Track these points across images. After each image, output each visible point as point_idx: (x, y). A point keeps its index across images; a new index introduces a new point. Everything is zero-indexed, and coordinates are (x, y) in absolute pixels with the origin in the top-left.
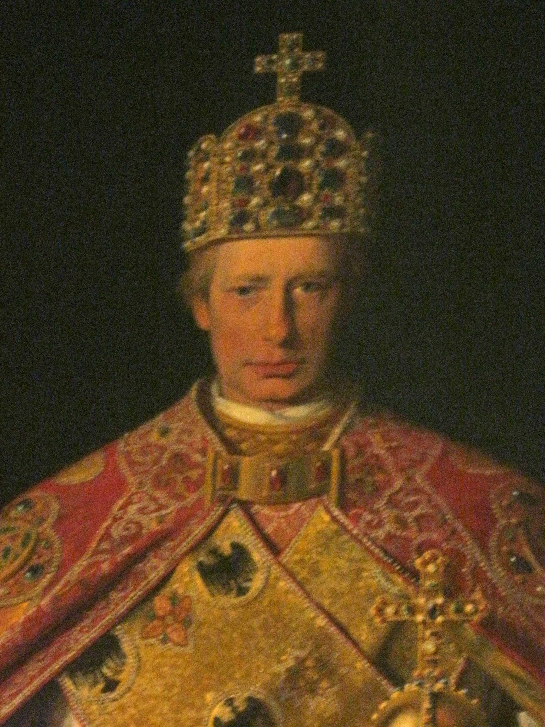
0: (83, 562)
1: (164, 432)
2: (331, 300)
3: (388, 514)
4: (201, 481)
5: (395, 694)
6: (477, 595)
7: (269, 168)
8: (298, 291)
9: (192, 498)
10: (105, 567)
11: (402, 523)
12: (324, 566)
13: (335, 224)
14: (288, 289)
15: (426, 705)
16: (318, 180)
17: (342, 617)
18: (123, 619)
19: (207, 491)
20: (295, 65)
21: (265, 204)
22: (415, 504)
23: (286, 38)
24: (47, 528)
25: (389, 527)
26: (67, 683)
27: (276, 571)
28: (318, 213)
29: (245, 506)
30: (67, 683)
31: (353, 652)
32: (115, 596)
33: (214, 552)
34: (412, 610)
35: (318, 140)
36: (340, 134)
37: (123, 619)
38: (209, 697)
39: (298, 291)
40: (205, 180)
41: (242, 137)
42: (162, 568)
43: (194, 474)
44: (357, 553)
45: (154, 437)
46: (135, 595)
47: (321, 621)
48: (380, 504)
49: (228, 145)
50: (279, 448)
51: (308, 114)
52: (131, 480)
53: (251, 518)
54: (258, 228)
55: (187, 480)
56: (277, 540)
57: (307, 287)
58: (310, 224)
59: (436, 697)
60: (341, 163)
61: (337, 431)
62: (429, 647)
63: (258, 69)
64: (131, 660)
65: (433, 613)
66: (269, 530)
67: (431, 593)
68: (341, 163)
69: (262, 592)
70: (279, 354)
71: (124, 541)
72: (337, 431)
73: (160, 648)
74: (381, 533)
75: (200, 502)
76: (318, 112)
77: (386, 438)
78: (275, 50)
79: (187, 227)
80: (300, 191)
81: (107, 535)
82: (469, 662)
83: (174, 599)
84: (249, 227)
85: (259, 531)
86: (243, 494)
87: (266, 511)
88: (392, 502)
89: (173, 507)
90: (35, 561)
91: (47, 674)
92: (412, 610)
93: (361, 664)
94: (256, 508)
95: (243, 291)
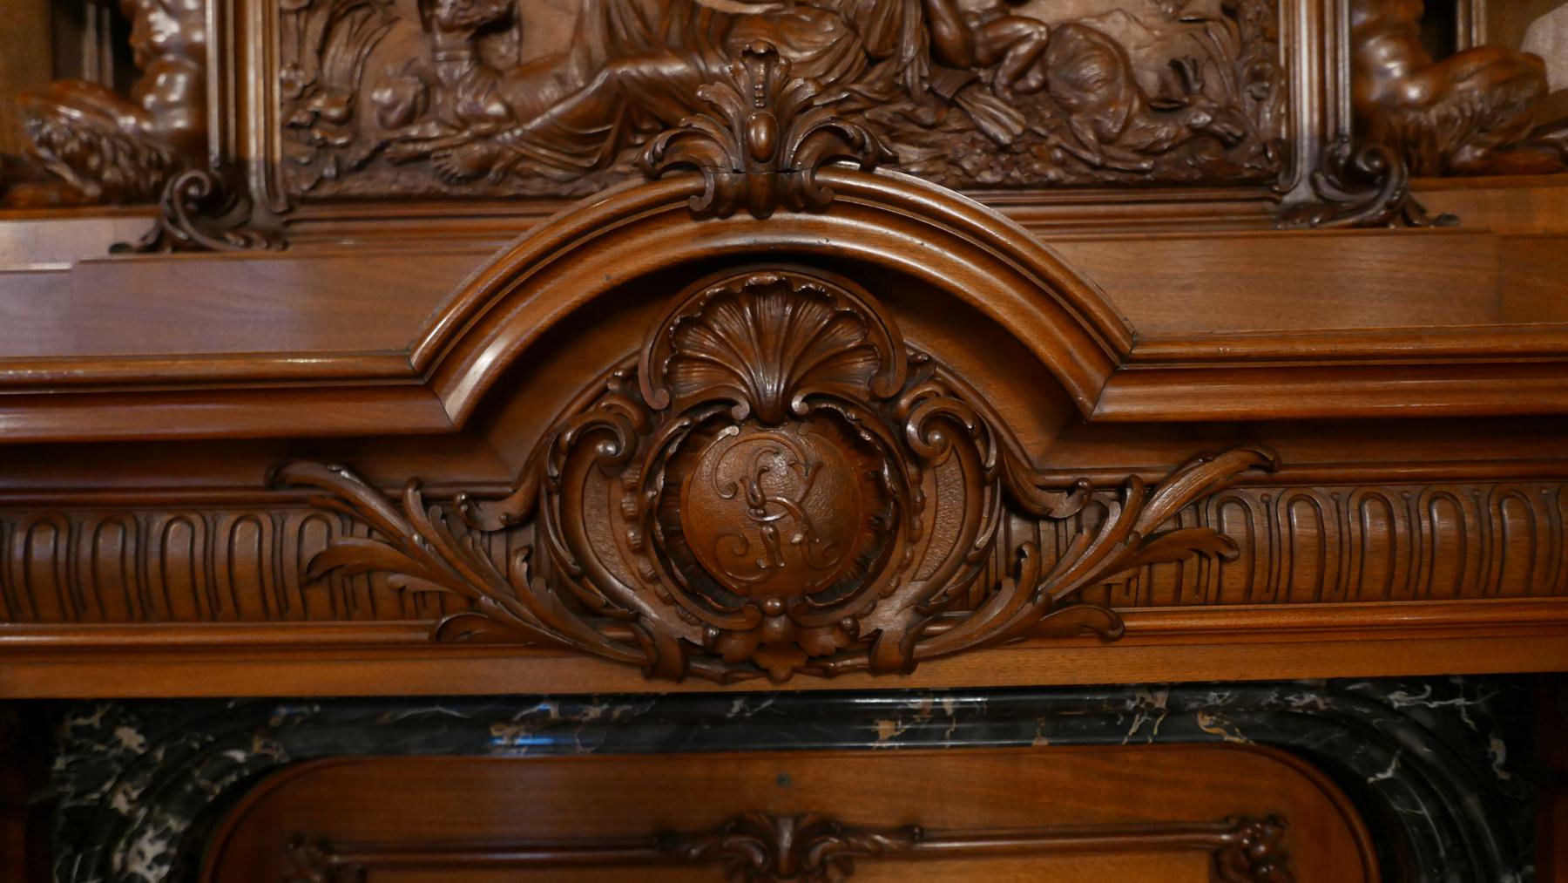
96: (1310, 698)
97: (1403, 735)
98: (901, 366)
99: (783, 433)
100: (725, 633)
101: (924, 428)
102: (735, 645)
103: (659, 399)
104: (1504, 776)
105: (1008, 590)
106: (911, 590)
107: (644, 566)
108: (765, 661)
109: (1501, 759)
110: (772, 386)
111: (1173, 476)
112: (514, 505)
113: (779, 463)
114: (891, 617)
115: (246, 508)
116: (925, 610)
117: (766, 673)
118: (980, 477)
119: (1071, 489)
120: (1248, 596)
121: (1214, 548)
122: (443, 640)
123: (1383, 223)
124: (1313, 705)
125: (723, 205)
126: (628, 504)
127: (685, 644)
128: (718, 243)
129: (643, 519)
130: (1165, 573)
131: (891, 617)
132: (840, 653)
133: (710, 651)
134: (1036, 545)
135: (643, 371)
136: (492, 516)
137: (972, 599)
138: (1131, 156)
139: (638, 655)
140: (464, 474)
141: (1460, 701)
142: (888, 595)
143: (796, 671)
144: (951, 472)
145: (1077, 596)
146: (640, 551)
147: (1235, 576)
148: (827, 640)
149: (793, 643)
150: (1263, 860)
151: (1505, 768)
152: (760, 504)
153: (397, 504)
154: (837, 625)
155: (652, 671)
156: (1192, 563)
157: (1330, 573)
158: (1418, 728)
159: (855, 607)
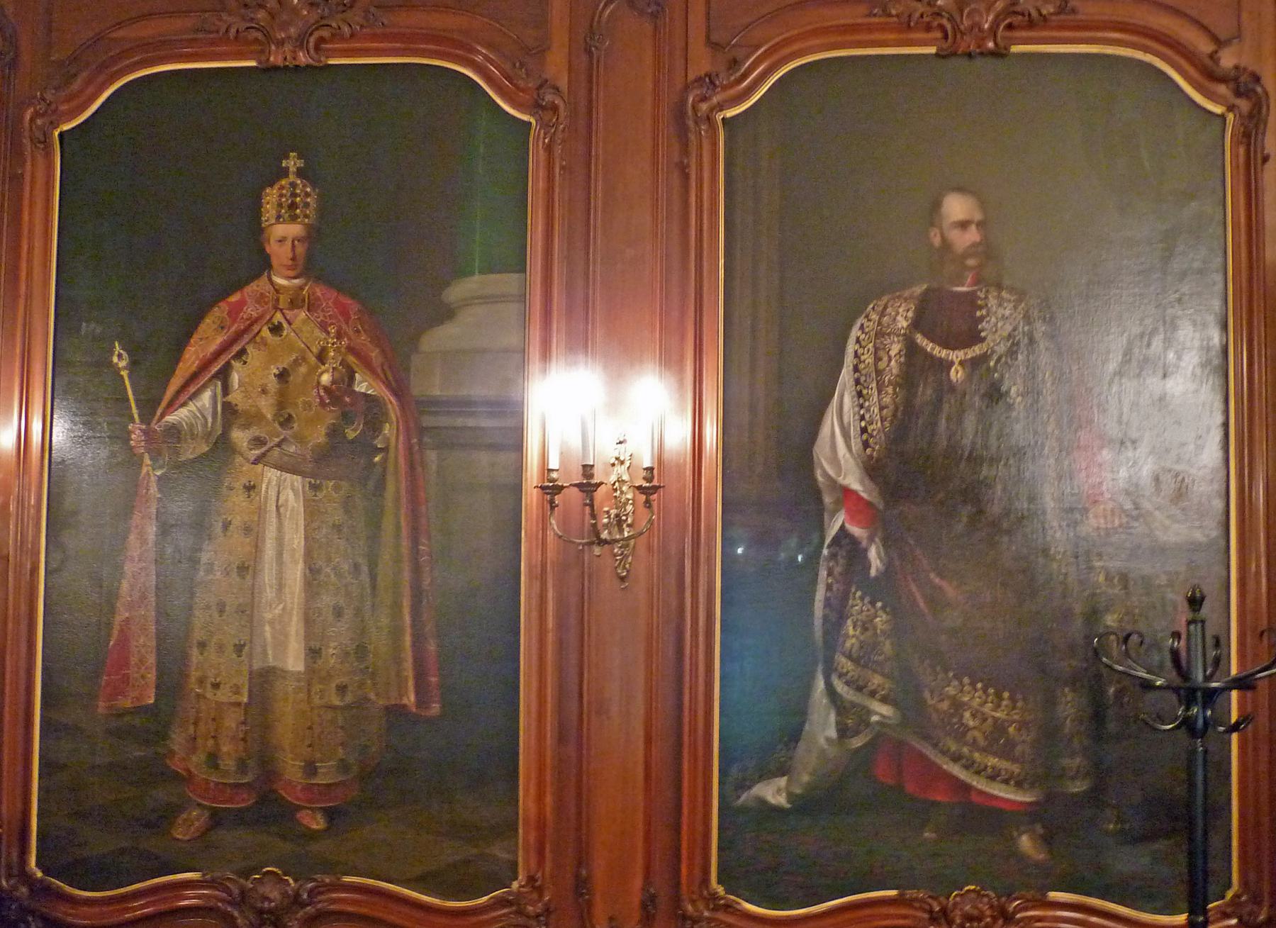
0: (236, 325)
1: (258, 286)
2: (306, 245)
3: (321, 314)
4: (269, 301)
5: (323, 367)
6: (346, 339)
7: (287, 200)
8: (296, 242)
9: (266, 307)
10: (242, 327)
11: (325, 317)
12: (304, 329)
13: (306, 220)
14: (293, 241)
15: (331, 370)
16: (302, 205)
17: (309, 345)
18: (248, 343)
19: (270, 305)
20: (295, 164)
21: (286, 212)
22: (329, 311)
23: (292, 154)
24: (225, 315)
25: (321, 318)
26: (233, 362)
27: (290, 330)
28: (302, 216)
29: (281, 310)
30: (233, 362)
31: (310, 355)
32: (245, 336)
33: (273, 324)
34: (328, 343)
35: (302, 191)
36: (308, 190)
37: (248, 343)
38: (272, 367)
39: (296, 242)
40: (268, 203)
41: (279, 189)
42: (258, 329)
43: (266, 300)
44: (313, 325)
45: (255, 288)
46: (251, 335)
47: (303, 346)
48: (319, 311)
49: (275, 191)
50: (291, 293)
51: (299, 182)
52: (249, 301)
53: (283, 314)
54: (284, 220)
55: (264, 302)
56: (291, 321)
57: (299, 241)
58: (299, 220)
59: (334, 368)
60: (309, 200)
61: (307, 288)
62: (332, 354)
63: (283, 165)
64: (250, 355)
65: (333, 344)
66: (288, 318)
67: (333, 338)
68: (309, 200)
69: (286, 336)
70: (290, 263)
71: (247, 319)
72: (307, 288)
73: (258, 352)
74: (319, 320)
75: (268, 308)
76: (302, 182)
77: (321, 290)
78: (287, 158)
79: (263, 219)
80: (297, 208)
81: (242, 318)
82: (343, 360)
83: (262, 338)
84: (281, 220)
85: (285, 318)
86: (281, 307)
87: (287, 312)
88: (323, 311)
89: (261, 310)
90: (222, 325)
91: (227, 359)
92: (328, 343)
93: (314, 359)
94: (284, 311)
95: (280, 241)
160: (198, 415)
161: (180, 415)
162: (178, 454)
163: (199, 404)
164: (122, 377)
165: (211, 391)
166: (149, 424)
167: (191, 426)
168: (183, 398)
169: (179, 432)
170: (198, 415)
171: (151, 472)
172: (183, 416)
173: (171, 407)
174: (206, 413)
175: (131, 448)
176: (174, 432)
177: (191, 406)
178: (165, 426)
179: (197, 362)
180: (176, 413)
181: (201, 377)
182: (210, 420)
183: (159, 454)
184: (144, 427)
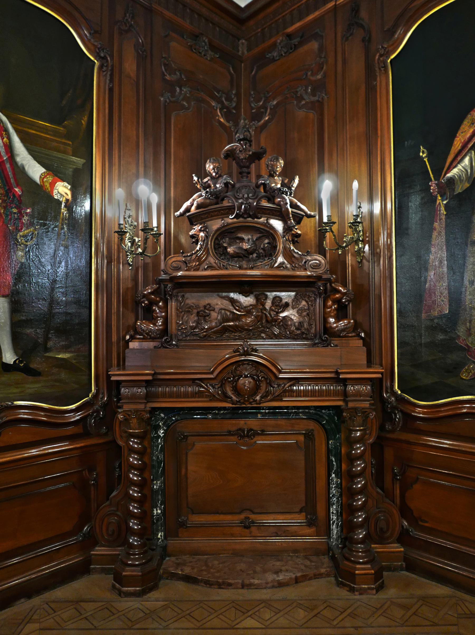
96: (312, 411)
97: (324, 416)
98: (259, 371)
99: (247, 379)
100: (241, 399)
101: (262, 378)
102: (242, 401)
103: (235, 375)
104: (337, 422)
105: (270, 395)
106: (260, 395)
107: (233, 392)
108: (245, 403)
109: (336, 419)
110: (246, 374)
111: (288, 383)
112: (219, 385)
113: (247, 381)
114: (258, 398)
115: (190, 386)
116: (262, 397)
117: (245, 404)
118: (267, 383)
119: (277, 384)
120: (296, 396)
121: (292, 391)
122: (211, 401)
123: (327, 346)
124: (313, 412)
125: (242, 355)
126: (231, 386)
127: (237, 401)
128: (241, 359)
129: (233, 387)
130: (287, 394)
131: (258, 398)
132: (253, 402)
133: (239, 402)
134: (274, 390)
135: (233, 371)
136: (217, 387)
137: (266, 396)
138: (293, 335)
139: (232, 402)
140: (214, 382)
141: (331, 412)
142: (258, 396)
143: (248, 404)
144: (265, 382)
145: (278, 396)
146: (232, 391)
147: (295, 394)
148: (251, 400)
149: (248, 401)
150: (310, 435)
151: (337, 420)
152: (245, 386)
153: (207, 385)
154: (253, 399)
155: (232, 404)
156: (290, 393)
157: (305, 394)
158: (326, 415)
159: (255, 397)
160: (463, 170)
161: (455, 171)
162: (454, 190)
163: (463, 165)
164: (425, 161)
165: (469, 156)
166: (439, 180)
167: (460, 177)
168: (454, 164)
169: (454, 180)
170: (463, 170)
171: (442, 203)
172: (455, 172)
173: (449, 170)
174: (466, 168)
175: (431, 193)
176: (451, 181)
177: (460, 167)
178: (447, 179)
179: (461, 144)
180: (452, 172)
181: (463, 151)
182: (469, 171)
183: (445, 193)
184: (436, 182)
